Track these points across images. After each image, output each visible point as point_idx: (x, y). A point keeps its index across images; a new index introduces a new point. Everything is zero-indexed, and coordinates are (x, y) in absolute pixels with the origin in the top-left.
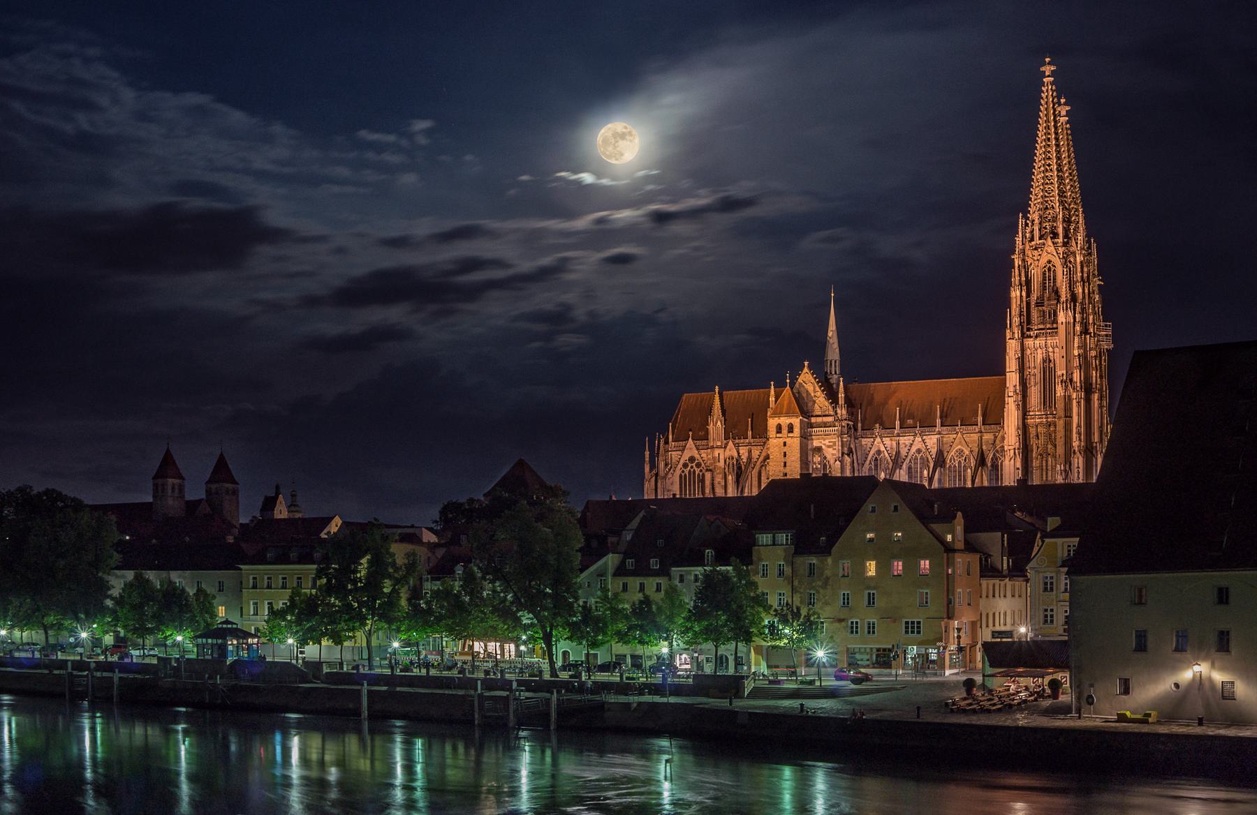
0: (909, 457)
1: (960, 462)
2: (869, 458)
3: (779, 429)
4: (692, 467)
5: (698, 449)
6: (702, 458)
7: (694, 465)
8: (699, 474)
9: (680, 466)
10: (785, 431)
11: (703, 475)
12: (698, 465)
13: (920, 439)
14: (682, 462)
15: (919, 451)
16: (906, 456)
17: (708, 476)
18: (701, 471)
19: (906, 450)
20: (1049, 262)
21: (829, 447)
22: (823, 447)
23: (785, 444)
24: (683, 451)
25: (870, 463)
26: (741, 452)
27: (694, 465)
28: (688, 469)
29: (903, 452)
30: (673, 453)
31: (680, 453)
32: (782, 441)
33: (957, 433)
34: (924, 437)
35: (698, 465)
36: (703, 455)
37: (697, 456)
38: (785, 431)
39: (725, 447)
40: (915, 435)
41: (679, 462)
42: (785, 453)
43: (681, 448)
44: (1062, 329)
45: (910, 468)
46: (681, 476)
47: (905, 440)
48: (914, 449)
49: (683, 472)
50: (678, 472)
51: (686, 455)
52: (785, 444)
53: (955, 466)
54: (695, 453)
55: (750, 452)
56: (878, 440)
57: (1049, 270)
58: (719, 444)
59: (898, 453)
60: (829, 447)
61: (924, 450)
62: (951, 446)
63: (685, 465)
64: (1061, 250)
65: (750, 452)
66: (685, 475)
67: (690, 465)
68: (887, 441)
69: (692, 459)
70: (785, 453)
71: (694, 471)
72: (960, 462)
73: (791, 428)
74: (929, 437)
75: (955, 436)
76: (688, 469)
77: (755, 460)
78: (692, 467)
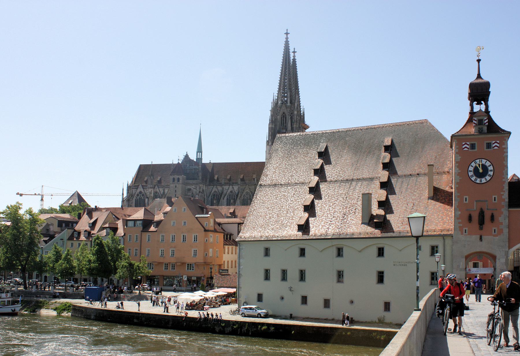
0: (227, 195)
1: (247, 197)
3: (174, 179)
4: (140, 196)
6: (145, 192)
7: (141, 195)
8: (143, 199)
9: (136, 195)
10: (176, 181)
11: (145, 200)
12: (143, 195)
13: (232, 187)
14: (136, 193)
15: (231, 192)
16: (226, 194)
17: (146, 200)
18: (144, 198)
19: (226, 191)
21: (194, 188)
22: (192, 188)
23: (176, 187)
24: (137, 189)
25: (212, 196)
26: (160, 190)
27: (141, 195)
28: (139, 197)
29: (225, 192)
30: (134, 190)
31: (136, 190)
32: (175, 185)
33: (246, 185)
34: (233, 186)
35: (143, 195)
36: (145, 191)
37: (143, 191)
38: (176, 181)
39: (154, 188)
40: (229, 185)
41: (135, 194)
42: (176, 191)
43: (136, 188)
45: (227, 199)
46: (136, 200)
47: (226, 187)
48: (229, 191)
49: (137, 198)
50: (135, 198)
51: (139, 190)
52: (176, 187)
53: (245, 199)
54: (142, 190)
55: (164, 190)
56: (215, 187)
59: (222, 193)
60: (194, 188)
61: (233, 192)
62: (244, 190)
63: (138, 195)
65: (164, 190)
66: (137, 200)
67: (140, 195)
69: (141, 192)
70: (176, 191)
72: (247, 197)
73: (178, 179)
74: (235, 186)
75: (245, 186)
76: (139, 197)
77: (166, 194)
78: (140, 196)
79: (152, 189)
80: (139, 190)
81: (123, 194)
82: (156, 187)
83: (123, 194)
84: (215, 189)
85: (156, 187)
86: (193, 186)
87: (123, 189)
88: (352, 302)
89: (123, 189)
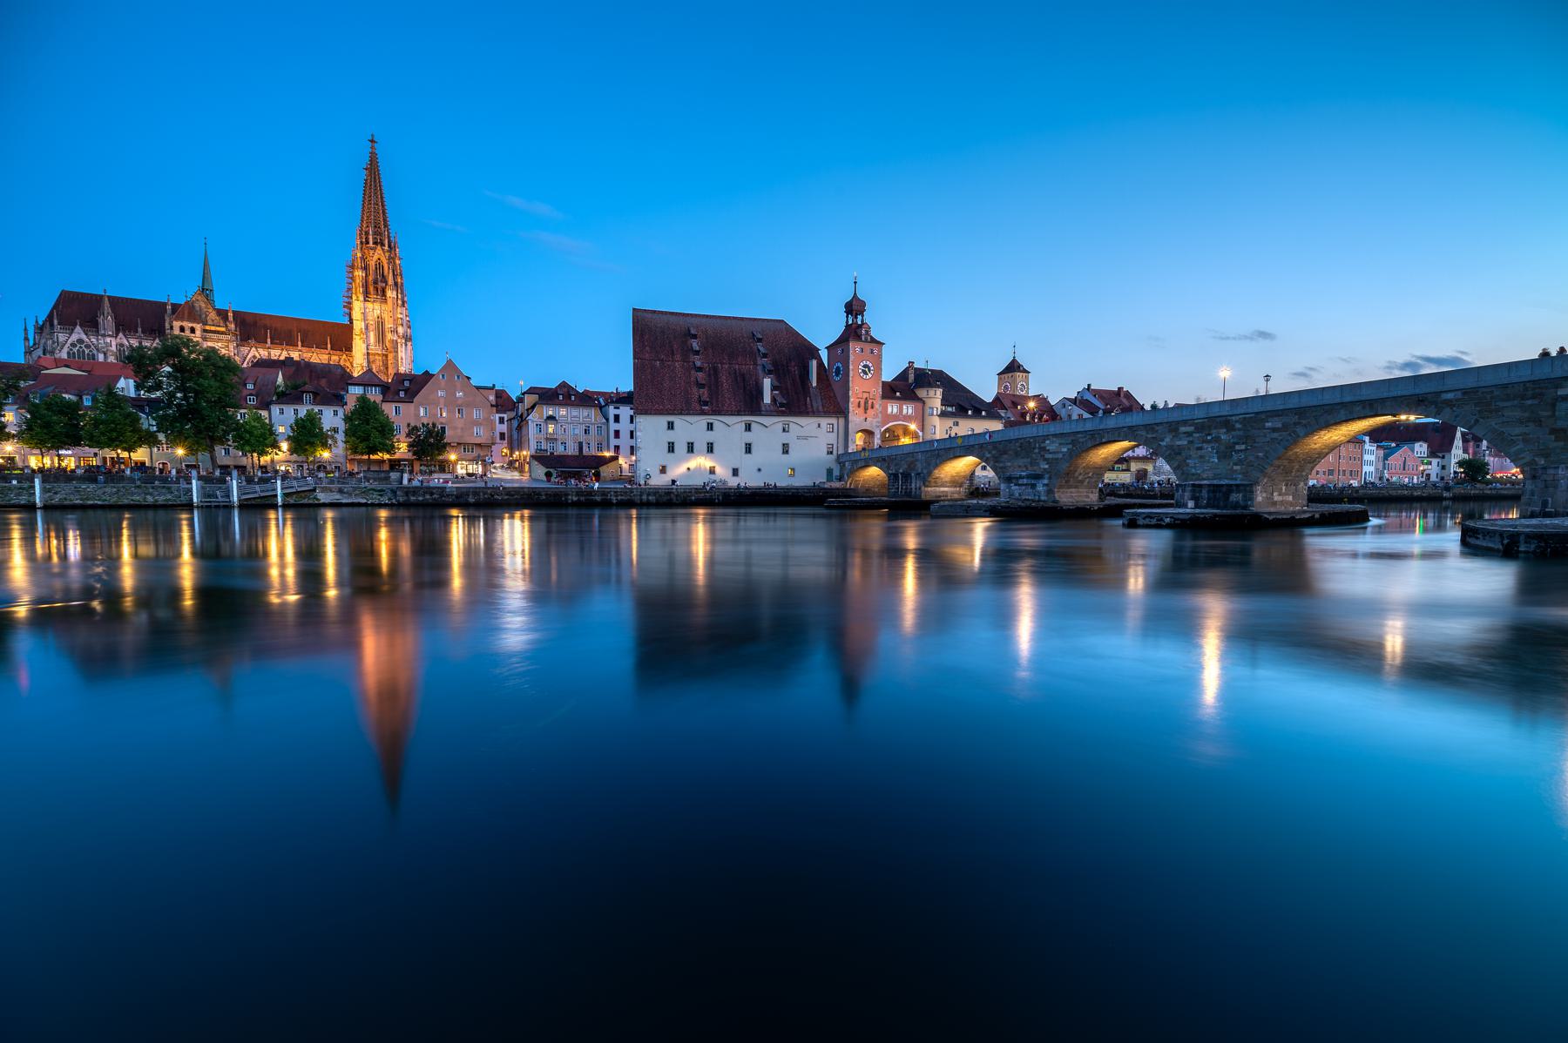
2: (248, 359)
4: (81, 347)
5: (86, 334)
9: (68, 345)
14: (70, 341)
20: (379, 259)
24: (71, 334)
39: (116, 337)
40: (282, 350)
44: (389, 301)
51: (74, 337)
56: (254, 349)
57: (379, 266)
58: (110, 333)
63: (73, 345)
64: (387, 254)
67: (79, 346)
68: (261, 351)
71: (84, 351)
79: (113, 339)
80: (74, 337)
81: (26, 339)
82: (121, 335)
83: (26, 339)
84: (253, 352)
85: (121, 335)
86: (220, 344)
87: (26, 329)
88: (759, 470)
89: (26, 329)
